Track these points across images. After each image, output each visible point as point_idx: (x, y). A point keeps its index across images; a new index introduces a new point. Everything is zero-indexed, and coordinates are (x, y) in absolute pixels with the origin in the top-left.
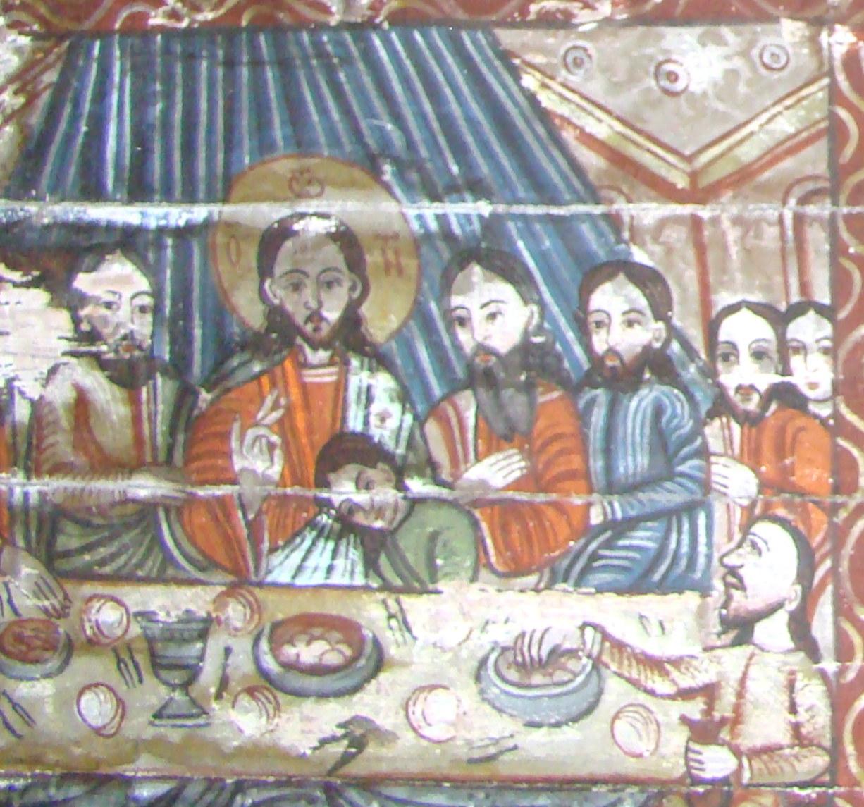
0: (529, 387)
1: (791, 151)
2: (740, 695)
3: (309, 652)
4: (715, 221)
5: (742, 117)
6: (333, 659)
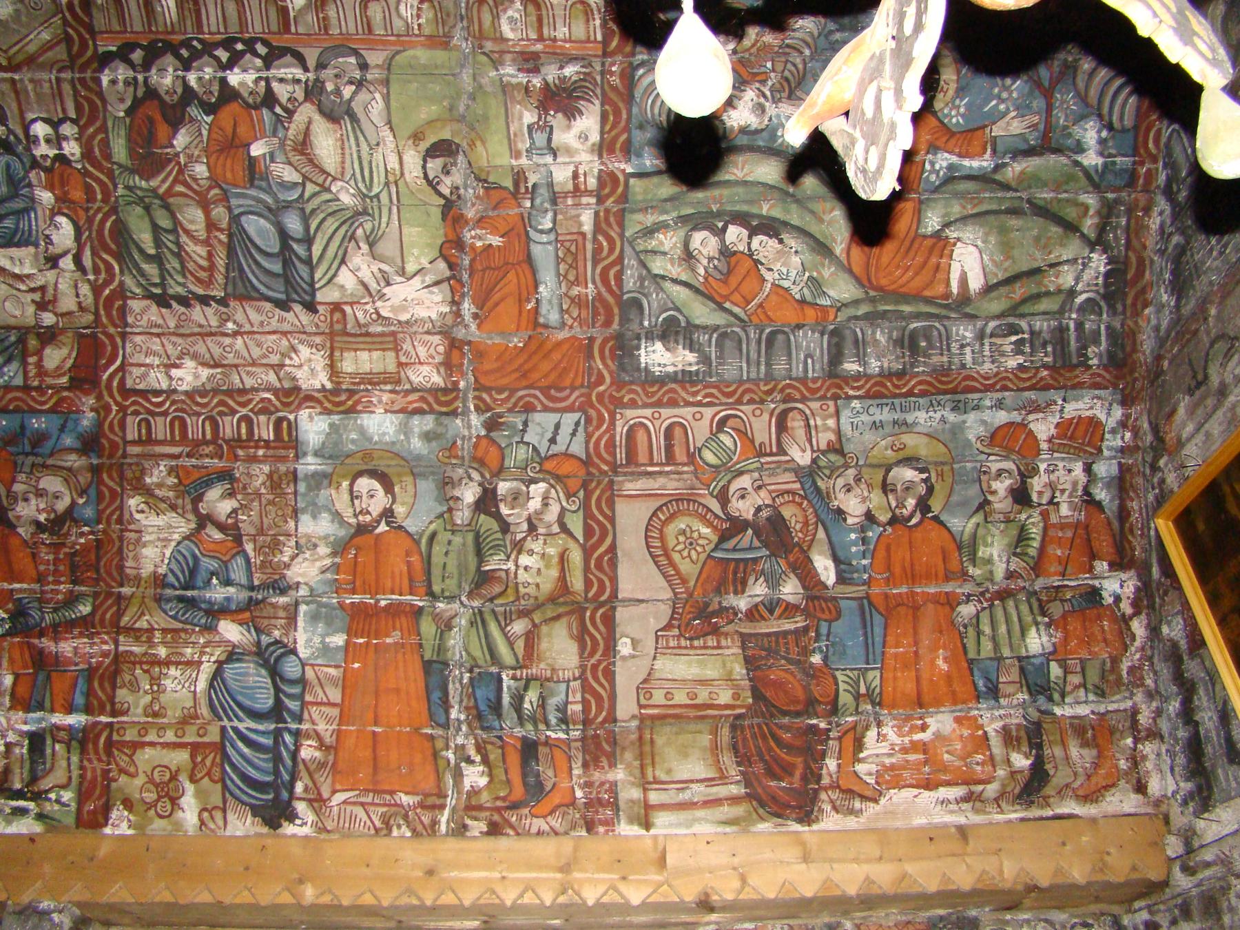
1: (51, 48)
4: (22, 80)
5: (24, 31)
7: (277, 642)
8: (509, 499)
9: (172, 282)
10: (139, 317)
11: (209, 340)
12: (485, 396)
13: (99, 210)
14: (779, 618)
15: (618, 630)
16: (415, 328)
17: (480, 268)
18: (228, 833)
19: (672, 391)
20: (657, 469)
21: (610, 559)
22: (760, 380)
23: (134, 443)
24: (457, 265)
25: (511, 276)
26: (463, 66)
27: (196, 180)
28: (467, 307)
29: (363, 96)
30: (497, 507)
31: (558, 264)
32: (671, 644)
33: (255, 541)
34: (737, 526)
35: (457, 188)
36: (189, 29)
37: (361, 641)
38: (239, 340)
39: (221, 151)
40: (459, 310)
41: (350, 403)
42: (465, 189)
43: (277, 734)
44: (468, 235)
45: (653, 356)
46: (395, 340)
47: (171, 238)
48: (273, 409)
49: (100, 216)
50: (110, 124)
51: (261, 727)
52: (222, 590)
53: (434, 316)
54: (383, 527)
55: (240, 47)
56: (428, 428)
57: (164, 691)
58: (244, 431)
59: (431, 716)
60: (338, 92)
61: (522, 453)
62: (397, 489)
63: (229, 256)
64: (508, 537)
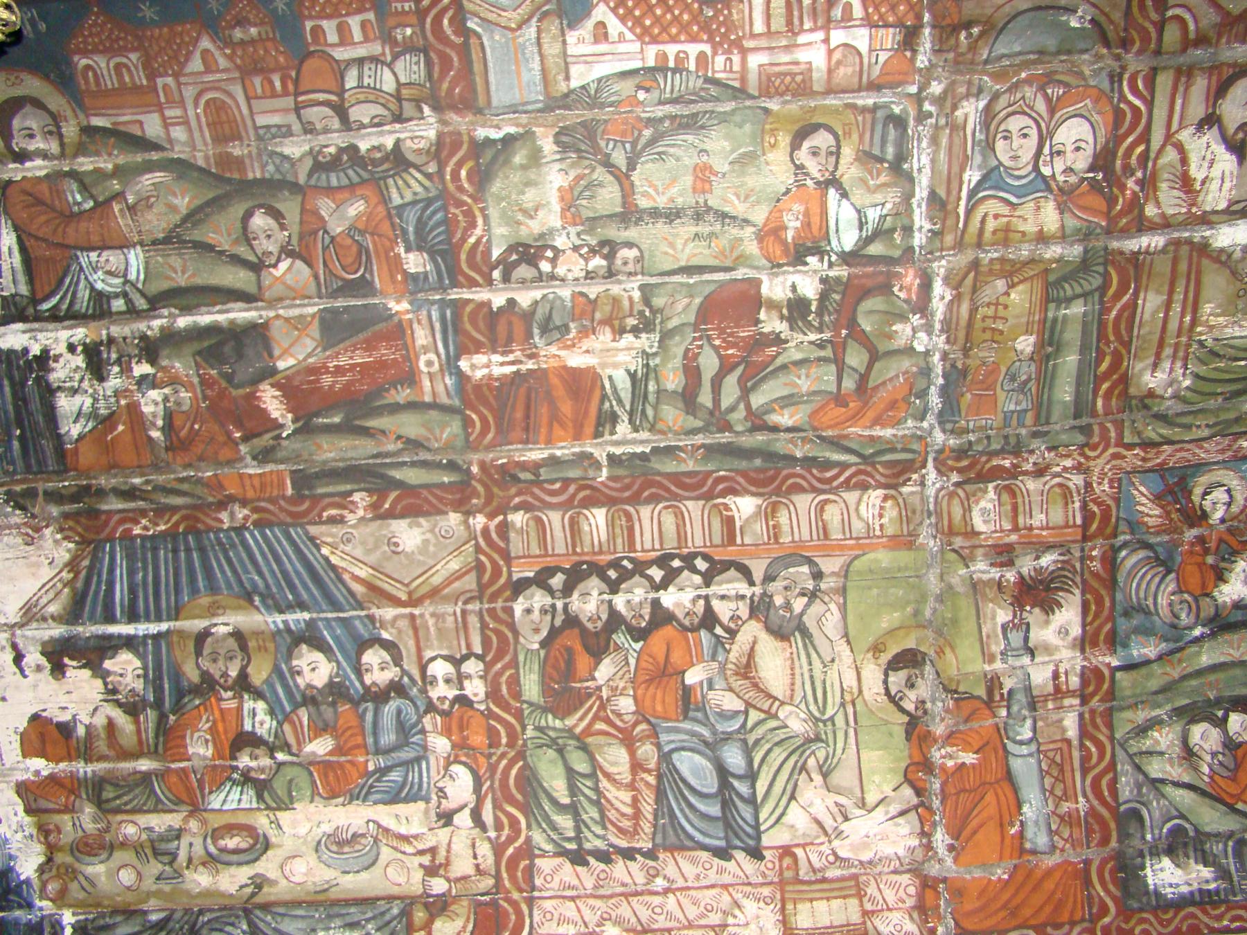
0: (334, 704)
1: (457, 579)
2: (448, 851)
3: (231, 843)
4: (422, 615)
5: (432, 563)
6: (244, 845)
9: (589, 835)
11: (634, 900)
13: (503, 755)
16: (879, 868)
25: (990, 797)
26: (929, 566)
27: (619, 715)
28: (941, 838)
29: (817, 608)
31: (1043, 778)
35: (923, 702)
36: (620, 548)
39: (650, 681)
40: (930, 842)
42: (933, 702)
44: (938, 755)
45: (1161, 875)
46: (857, 885)
49: (504, 762)
50: (521, 658)
53: (901, 852)
55: (676, 563)
60: (788, 606)
63: (657, 801)
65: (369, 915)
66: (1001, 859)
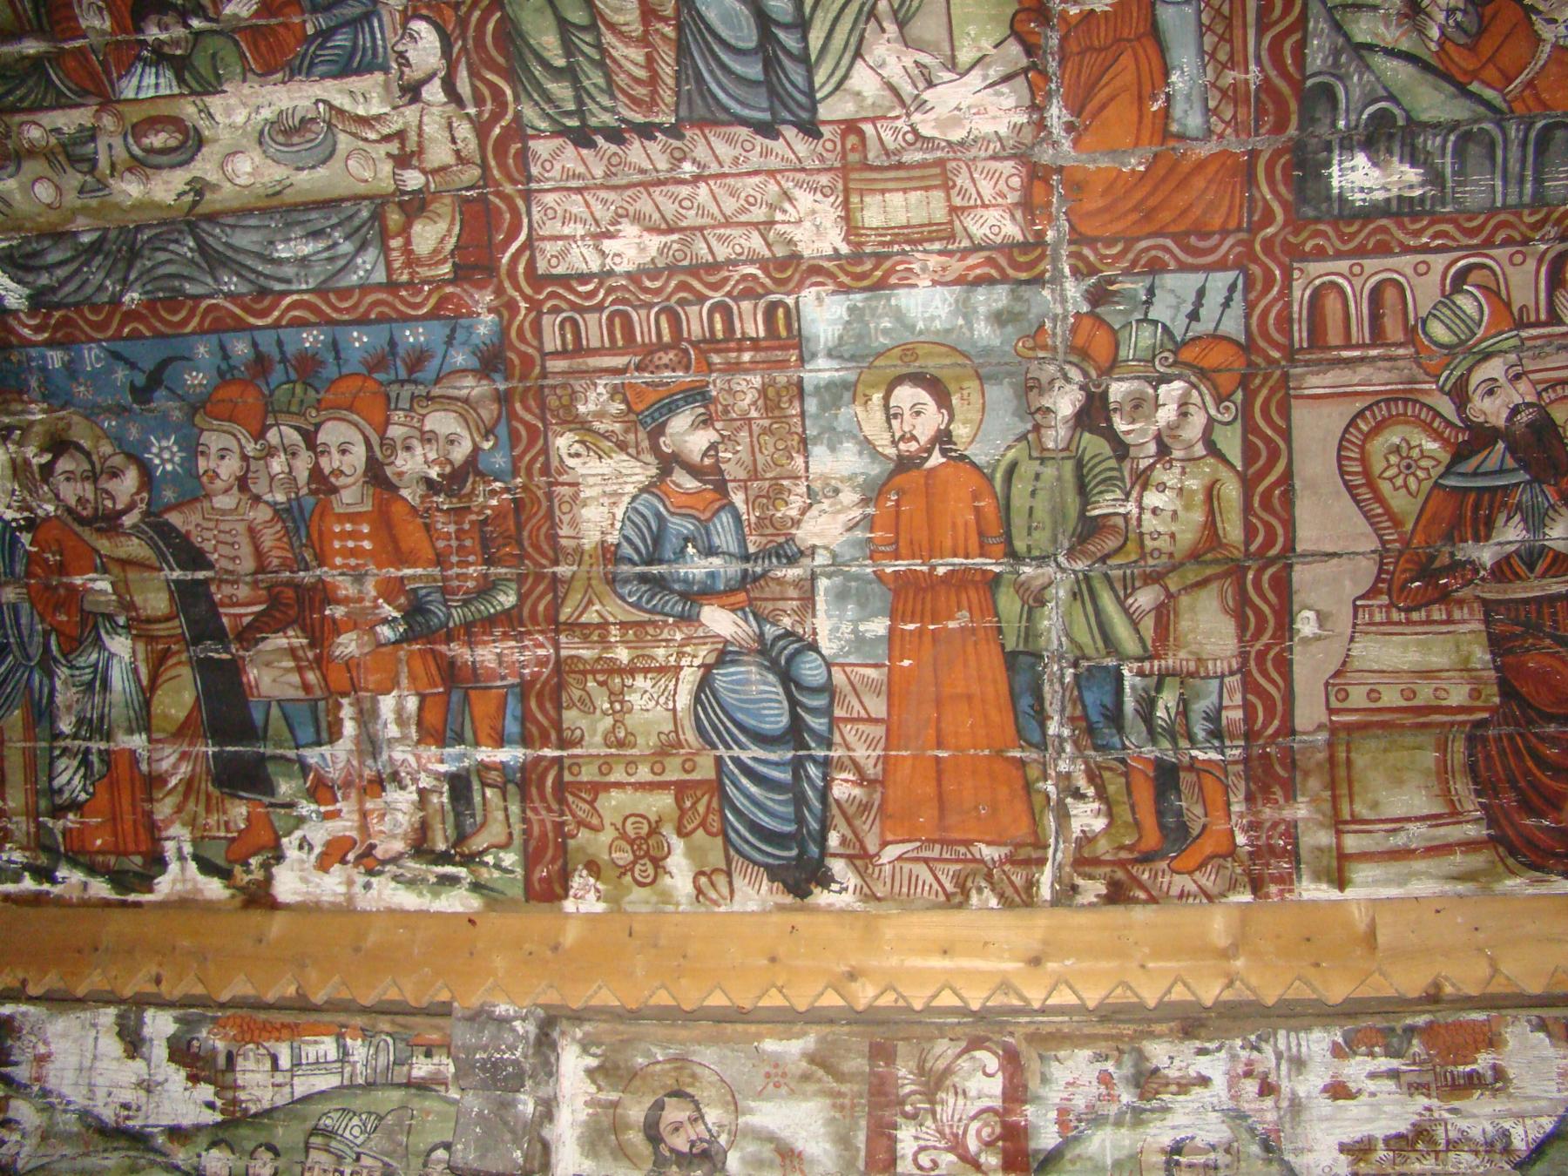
2: (420, 135)
3: (158, 140)
6: (173, 143)
7: (788, 634)
8: (1127, 408)
9: (593, 107)
10: (548, 165)
11: (656, 192)
12: (1086, 251)
14: (1543, 576)
15: (1296, 599)
16: (974, 152)
17: (1075, 49)
18: (736, 907)
19: (1384, 230)
20: (1357, 353)
21: (1284, 494)
22: (1525, 206)
23: (556, 354)
24: (1039, 47)
25: (1126, 59)
28: (1056, 113)
30: (1109, 420)
31: (1202, 35)
32: (1378, 618)
33: (746, 489)
34: (1480, 437)
37: (911, 627)
38: (703, 189)
40: (1043, 118)
41: (878, 273)
43: (797, 765)
45: (1351, 176)
47: (588, 38)
48: (760, 291)
49: (477, 14)
51: (773, 757)
52: (703, 562)
53: (1003, 131)
54: (936, 459)
56: (1000, 305)
57: (630, 711)
58: (719, 326)
59: (1019, 733)
61: (1145, 337)
62: (955, 400)
64: (1127, 465)
65: (334, 220)
66: (1136, 145)
